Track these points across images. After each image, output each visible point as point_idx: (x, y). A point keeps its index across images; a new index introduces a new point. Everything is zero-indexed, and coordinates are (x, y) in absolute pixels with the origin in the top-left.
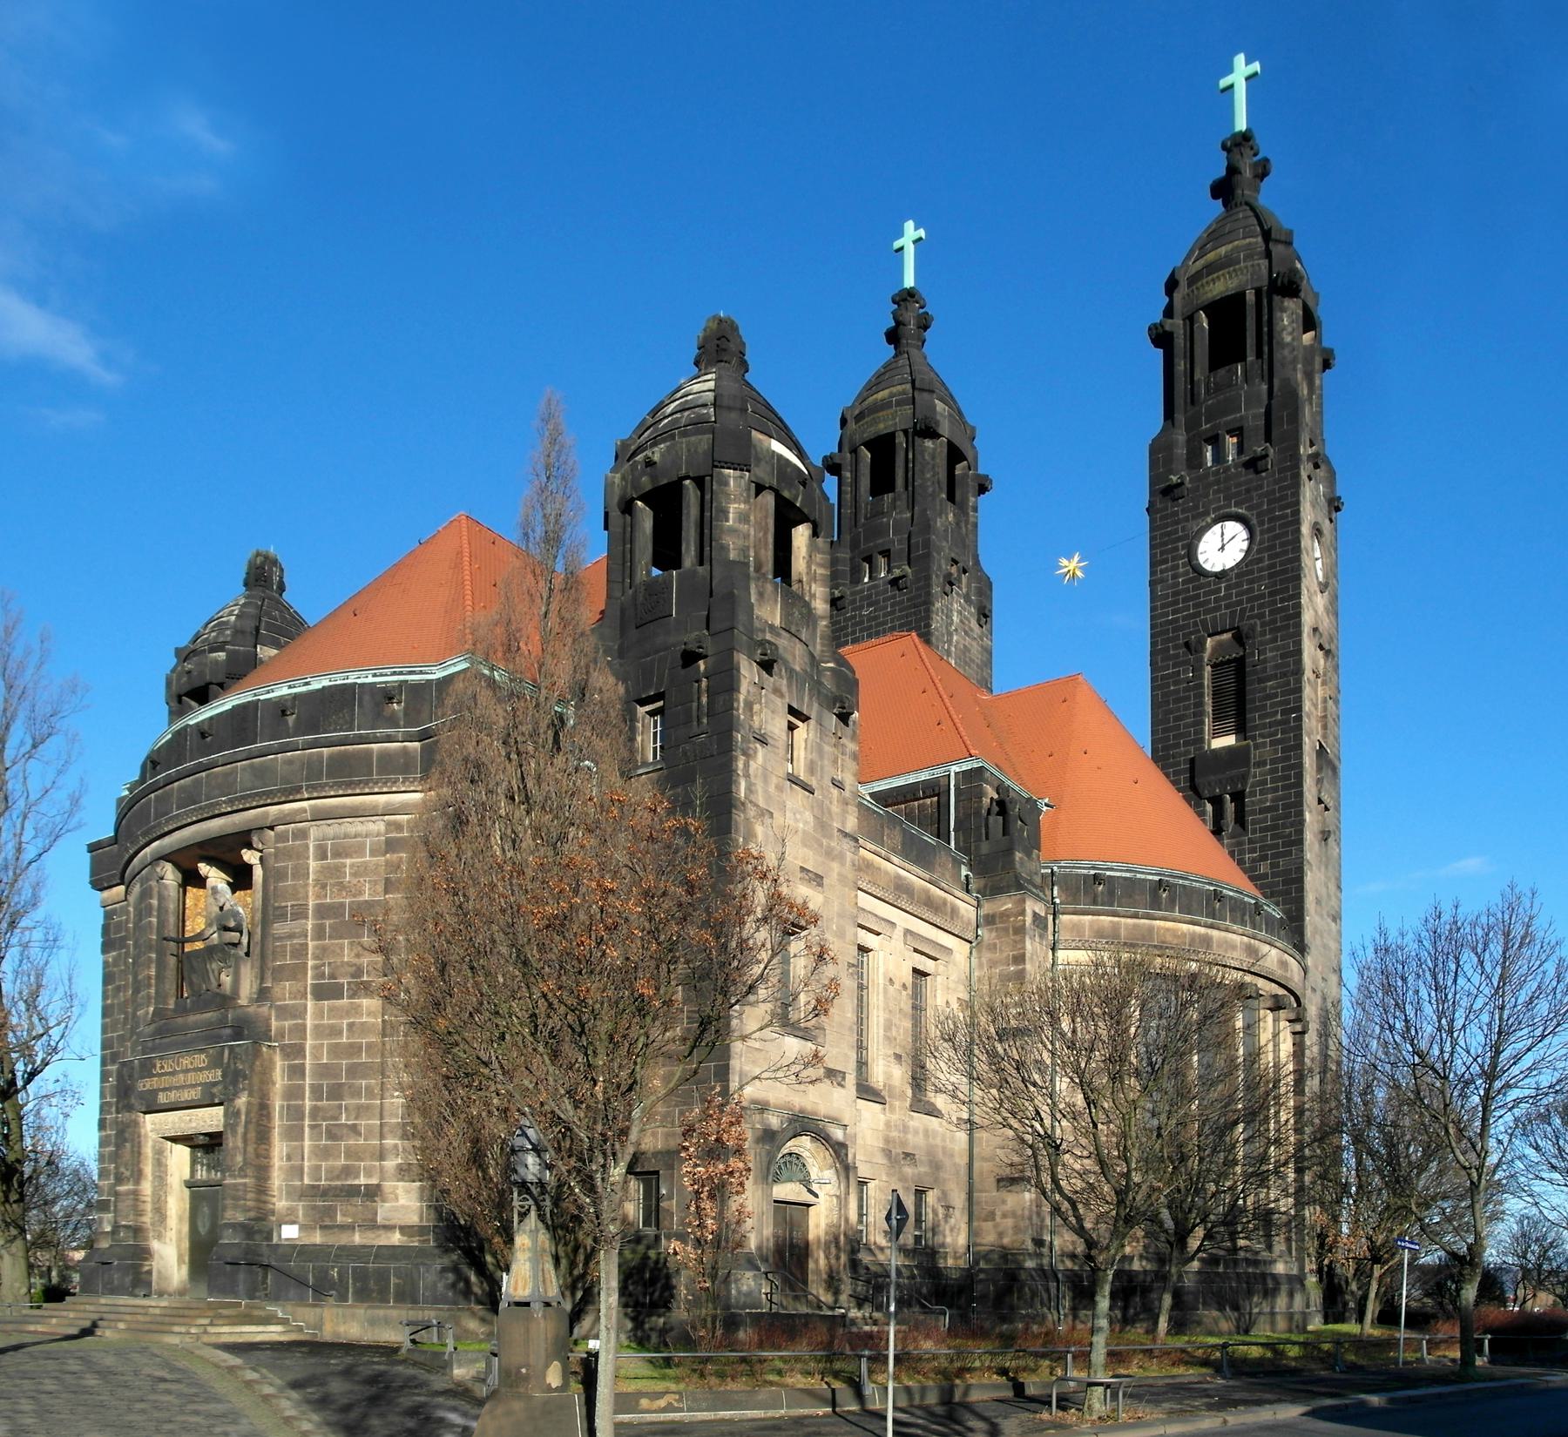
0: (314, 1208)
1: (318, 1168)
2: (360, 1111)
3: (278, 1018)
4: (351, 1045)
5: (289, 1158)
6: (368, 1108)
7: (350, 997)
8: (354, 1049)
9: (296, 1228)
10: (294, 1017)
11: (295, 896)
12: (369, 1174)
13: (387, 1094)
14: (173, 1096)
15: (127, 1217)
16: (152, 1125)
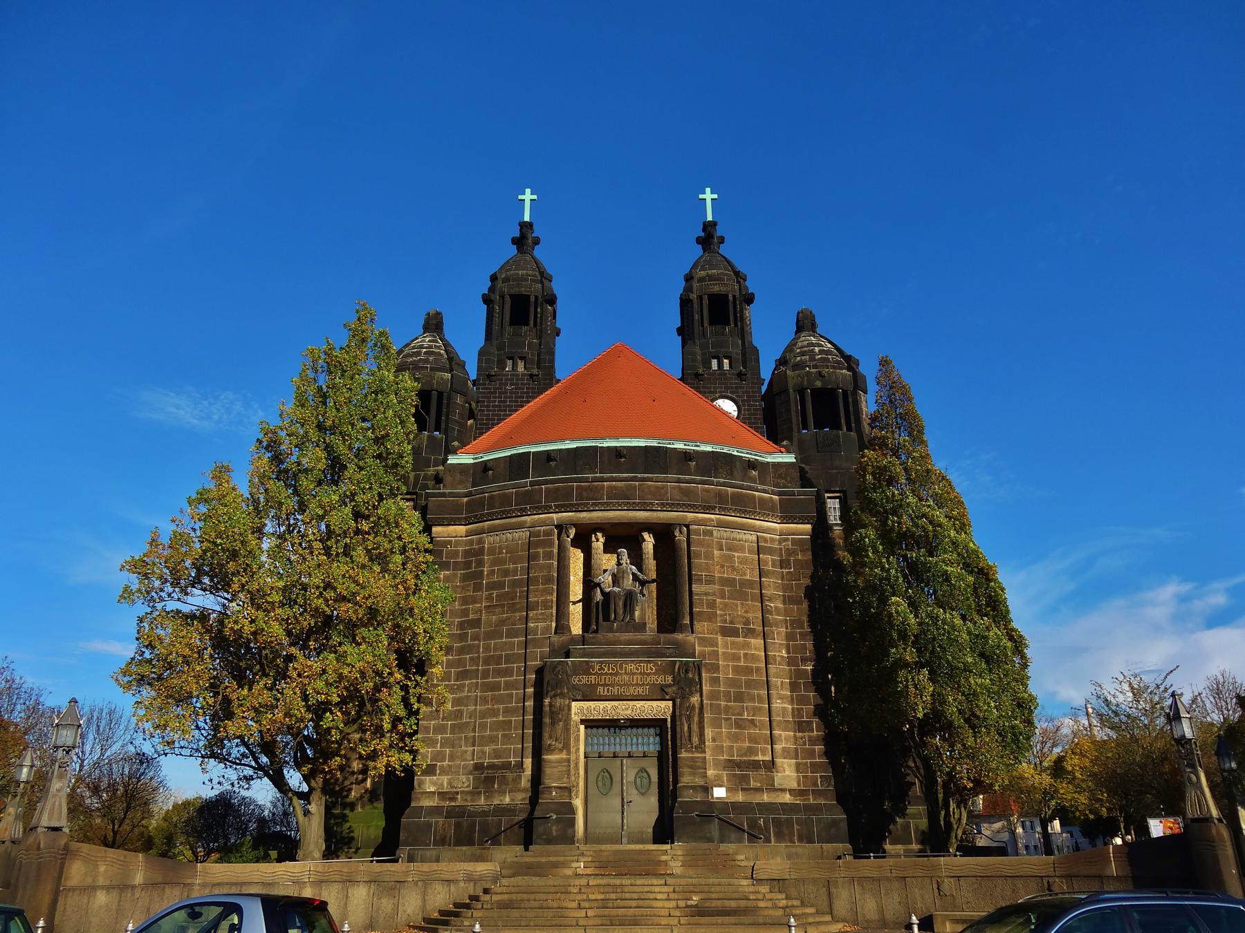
2: (756, 711)
3: (700, 645)
5: (714, 740)
6: (760, 709)
8: (748, 671)
10: (712, 646)
11: (708, 569)
12: (764, 754)
13: (773, 701)
14: (615, 690)
15: (559, 779)
16: (579, 709)
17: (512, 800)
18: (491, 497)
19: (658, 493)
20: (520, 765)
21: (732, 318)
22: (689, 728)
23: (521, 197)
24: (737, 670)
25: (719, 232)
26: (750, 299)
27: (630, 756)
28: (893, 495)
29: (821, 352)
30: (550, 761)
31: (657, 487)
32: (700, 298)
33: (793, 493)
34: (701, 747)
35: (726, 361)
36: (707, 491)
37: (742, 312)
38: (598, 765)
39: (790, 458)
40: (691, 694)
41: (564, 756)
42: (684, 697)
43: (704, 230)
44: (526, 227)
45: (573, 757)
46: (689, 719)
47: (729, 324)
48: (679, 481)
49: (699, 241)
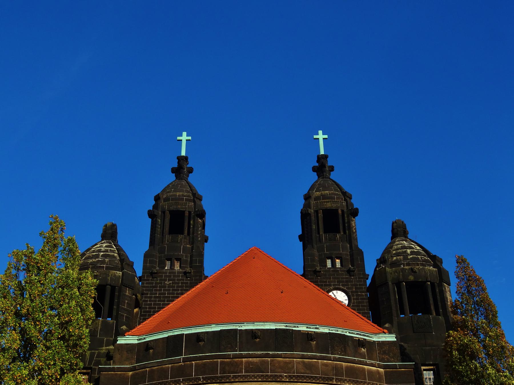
18: (151, 372)
19: (286, 367)
21: (341, 227)
23: (179, 138)
25: (330, 162)
26: (355, 213)
28: (476, 367)
29: (412, 253)
31: (286, 363)
32: (317, 212)
33: (395, 367)
35: (338, 261)
36: (326, 365)
37: (349, 223)
39: (391, 338)
43: (318, 162)
44: (183, 160)
47: (339, 232)
48: (303, 357)
49: (314, 169)
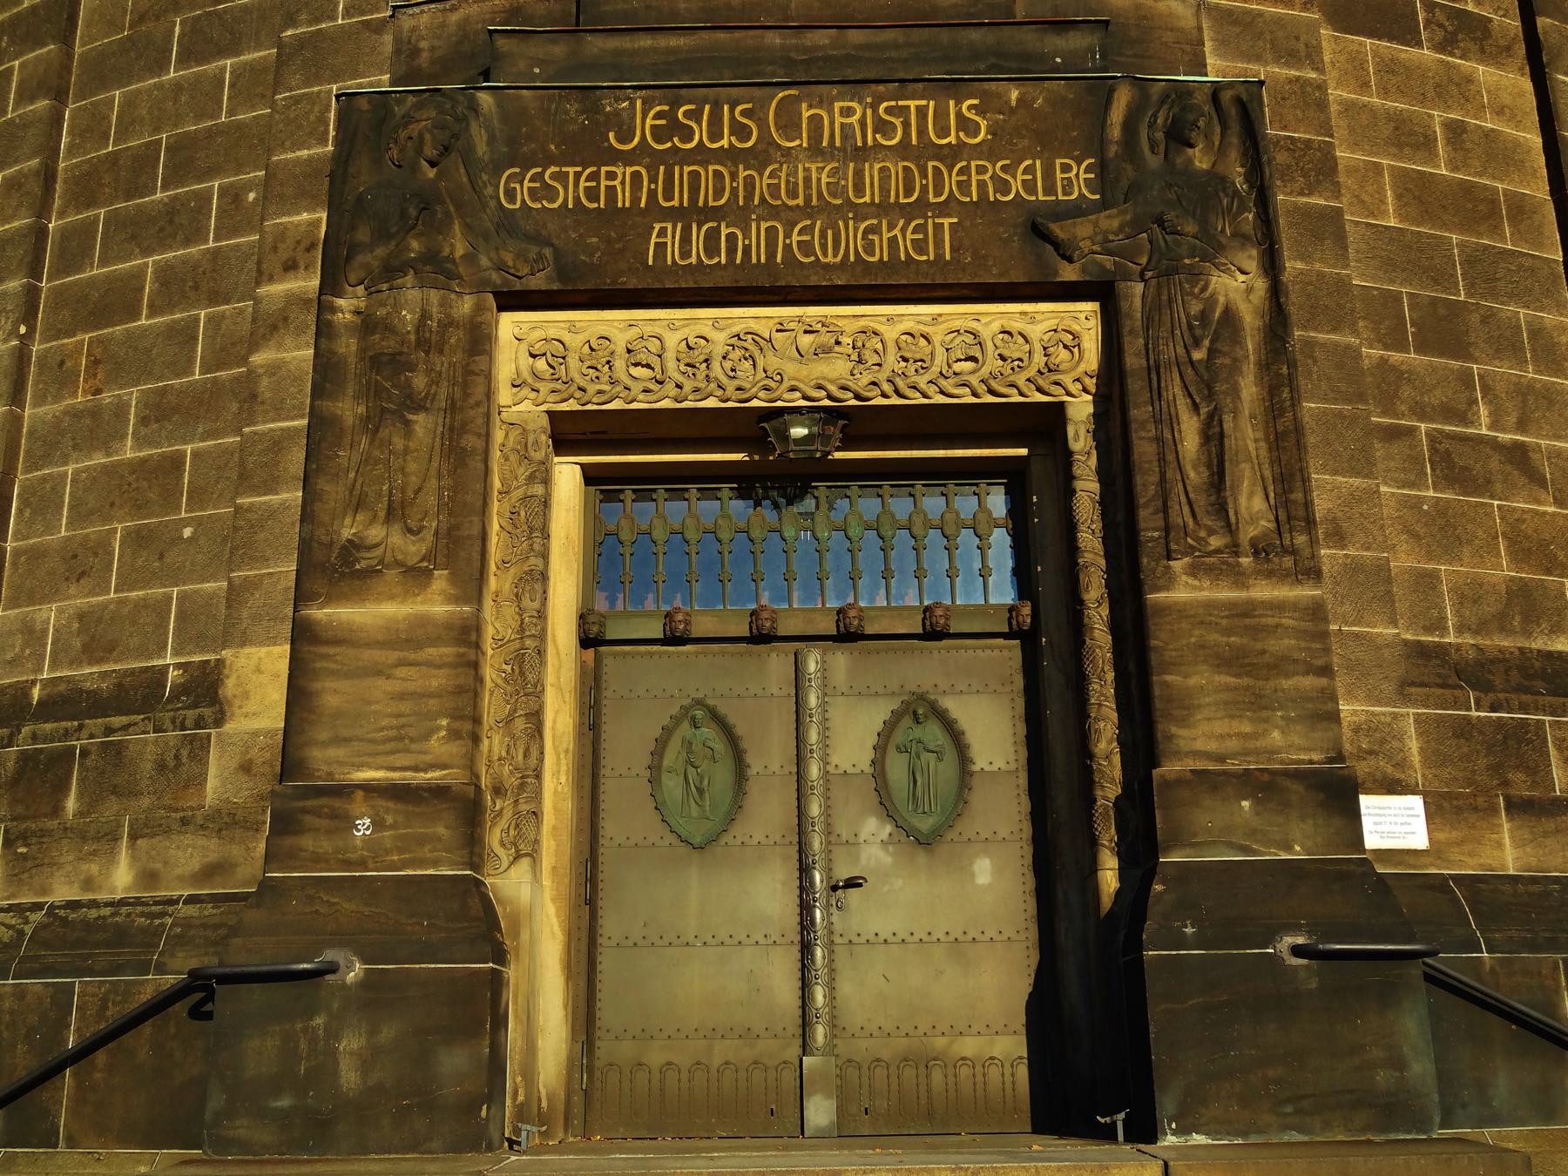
0: (1464, 729)
1: (1426, 582)
2: (1530, 405)
3: (1223, 45)
4: (1468, 189)
7: (1440, 47)
8: (1477, 209)
9: (1416, 802)
14: (755, 242)
15: (401, 739)
17: (149, 877)
20: (206, 691)
22: (1213, 436)
24: (1420, 195)
27: (847, 634)
30: (345, 638)
34: (1290, 541)
38: (656, 685)
40: (1212, 251)
41: (438, 603)
42: (1169, 271)
45: (497, 624)
46: (1209, 387)
